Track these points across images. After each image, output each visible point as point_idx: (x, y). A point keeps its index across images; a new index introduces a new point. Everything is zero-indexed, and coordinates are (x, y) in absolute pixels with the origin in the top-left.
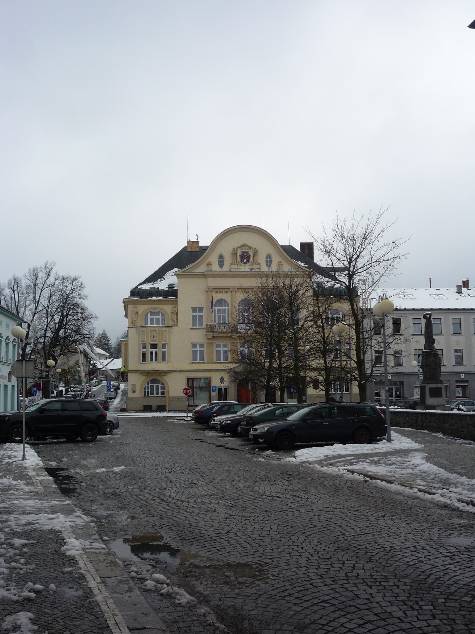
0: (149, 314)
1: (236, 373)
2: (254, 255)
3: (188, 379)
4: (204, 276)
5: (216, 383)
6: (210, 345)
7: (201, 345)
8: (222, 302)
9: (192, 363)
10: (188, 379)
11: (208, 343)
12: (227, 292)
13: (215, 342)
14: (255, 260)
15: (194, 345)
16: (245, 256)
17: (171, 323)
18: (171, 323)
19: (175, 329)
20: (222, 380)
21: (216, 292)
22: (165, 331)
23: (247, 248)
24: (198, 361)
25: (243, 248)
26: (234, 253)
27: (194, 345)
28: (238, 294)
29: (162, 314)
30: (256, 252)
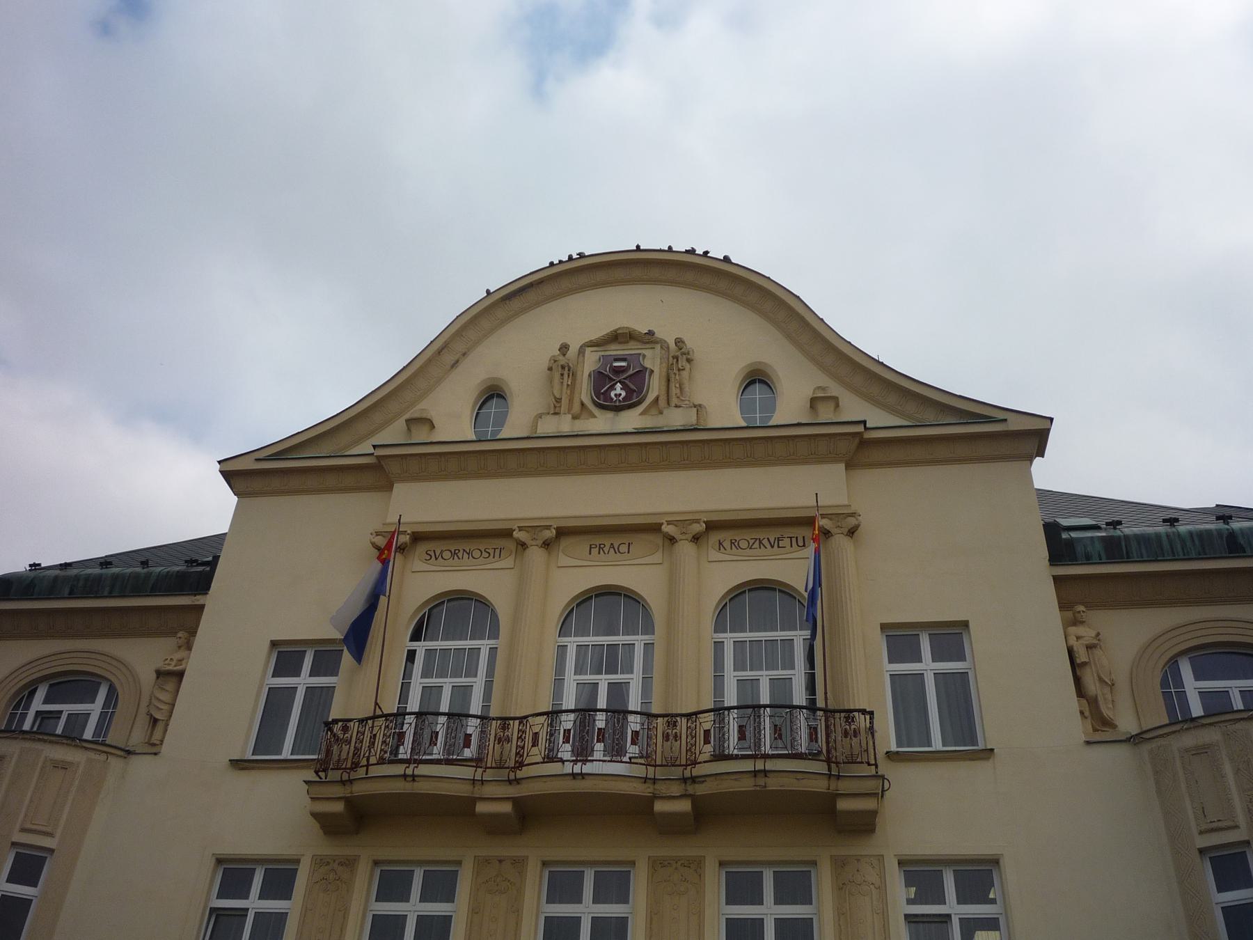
0: (41, 694)
2: (670, 368)
4: (379, 473)
6: (335, 874)
7: (280, 880)
8: (460, 611)
11: (320, 861)
13: (368, 852)
14: (674, 391)
15: (234, 875)
16: (618, 371)
17: (137, 738)
18: (137, 738)
19: (141, 766)
21: (431, 556)
22: (63, 766)
23: (632, 344)
25: (613, 347)
26: (562, 368)
27: (234, 875)
28: (564, 560)
29: (112, 691)
30: (680, 357)
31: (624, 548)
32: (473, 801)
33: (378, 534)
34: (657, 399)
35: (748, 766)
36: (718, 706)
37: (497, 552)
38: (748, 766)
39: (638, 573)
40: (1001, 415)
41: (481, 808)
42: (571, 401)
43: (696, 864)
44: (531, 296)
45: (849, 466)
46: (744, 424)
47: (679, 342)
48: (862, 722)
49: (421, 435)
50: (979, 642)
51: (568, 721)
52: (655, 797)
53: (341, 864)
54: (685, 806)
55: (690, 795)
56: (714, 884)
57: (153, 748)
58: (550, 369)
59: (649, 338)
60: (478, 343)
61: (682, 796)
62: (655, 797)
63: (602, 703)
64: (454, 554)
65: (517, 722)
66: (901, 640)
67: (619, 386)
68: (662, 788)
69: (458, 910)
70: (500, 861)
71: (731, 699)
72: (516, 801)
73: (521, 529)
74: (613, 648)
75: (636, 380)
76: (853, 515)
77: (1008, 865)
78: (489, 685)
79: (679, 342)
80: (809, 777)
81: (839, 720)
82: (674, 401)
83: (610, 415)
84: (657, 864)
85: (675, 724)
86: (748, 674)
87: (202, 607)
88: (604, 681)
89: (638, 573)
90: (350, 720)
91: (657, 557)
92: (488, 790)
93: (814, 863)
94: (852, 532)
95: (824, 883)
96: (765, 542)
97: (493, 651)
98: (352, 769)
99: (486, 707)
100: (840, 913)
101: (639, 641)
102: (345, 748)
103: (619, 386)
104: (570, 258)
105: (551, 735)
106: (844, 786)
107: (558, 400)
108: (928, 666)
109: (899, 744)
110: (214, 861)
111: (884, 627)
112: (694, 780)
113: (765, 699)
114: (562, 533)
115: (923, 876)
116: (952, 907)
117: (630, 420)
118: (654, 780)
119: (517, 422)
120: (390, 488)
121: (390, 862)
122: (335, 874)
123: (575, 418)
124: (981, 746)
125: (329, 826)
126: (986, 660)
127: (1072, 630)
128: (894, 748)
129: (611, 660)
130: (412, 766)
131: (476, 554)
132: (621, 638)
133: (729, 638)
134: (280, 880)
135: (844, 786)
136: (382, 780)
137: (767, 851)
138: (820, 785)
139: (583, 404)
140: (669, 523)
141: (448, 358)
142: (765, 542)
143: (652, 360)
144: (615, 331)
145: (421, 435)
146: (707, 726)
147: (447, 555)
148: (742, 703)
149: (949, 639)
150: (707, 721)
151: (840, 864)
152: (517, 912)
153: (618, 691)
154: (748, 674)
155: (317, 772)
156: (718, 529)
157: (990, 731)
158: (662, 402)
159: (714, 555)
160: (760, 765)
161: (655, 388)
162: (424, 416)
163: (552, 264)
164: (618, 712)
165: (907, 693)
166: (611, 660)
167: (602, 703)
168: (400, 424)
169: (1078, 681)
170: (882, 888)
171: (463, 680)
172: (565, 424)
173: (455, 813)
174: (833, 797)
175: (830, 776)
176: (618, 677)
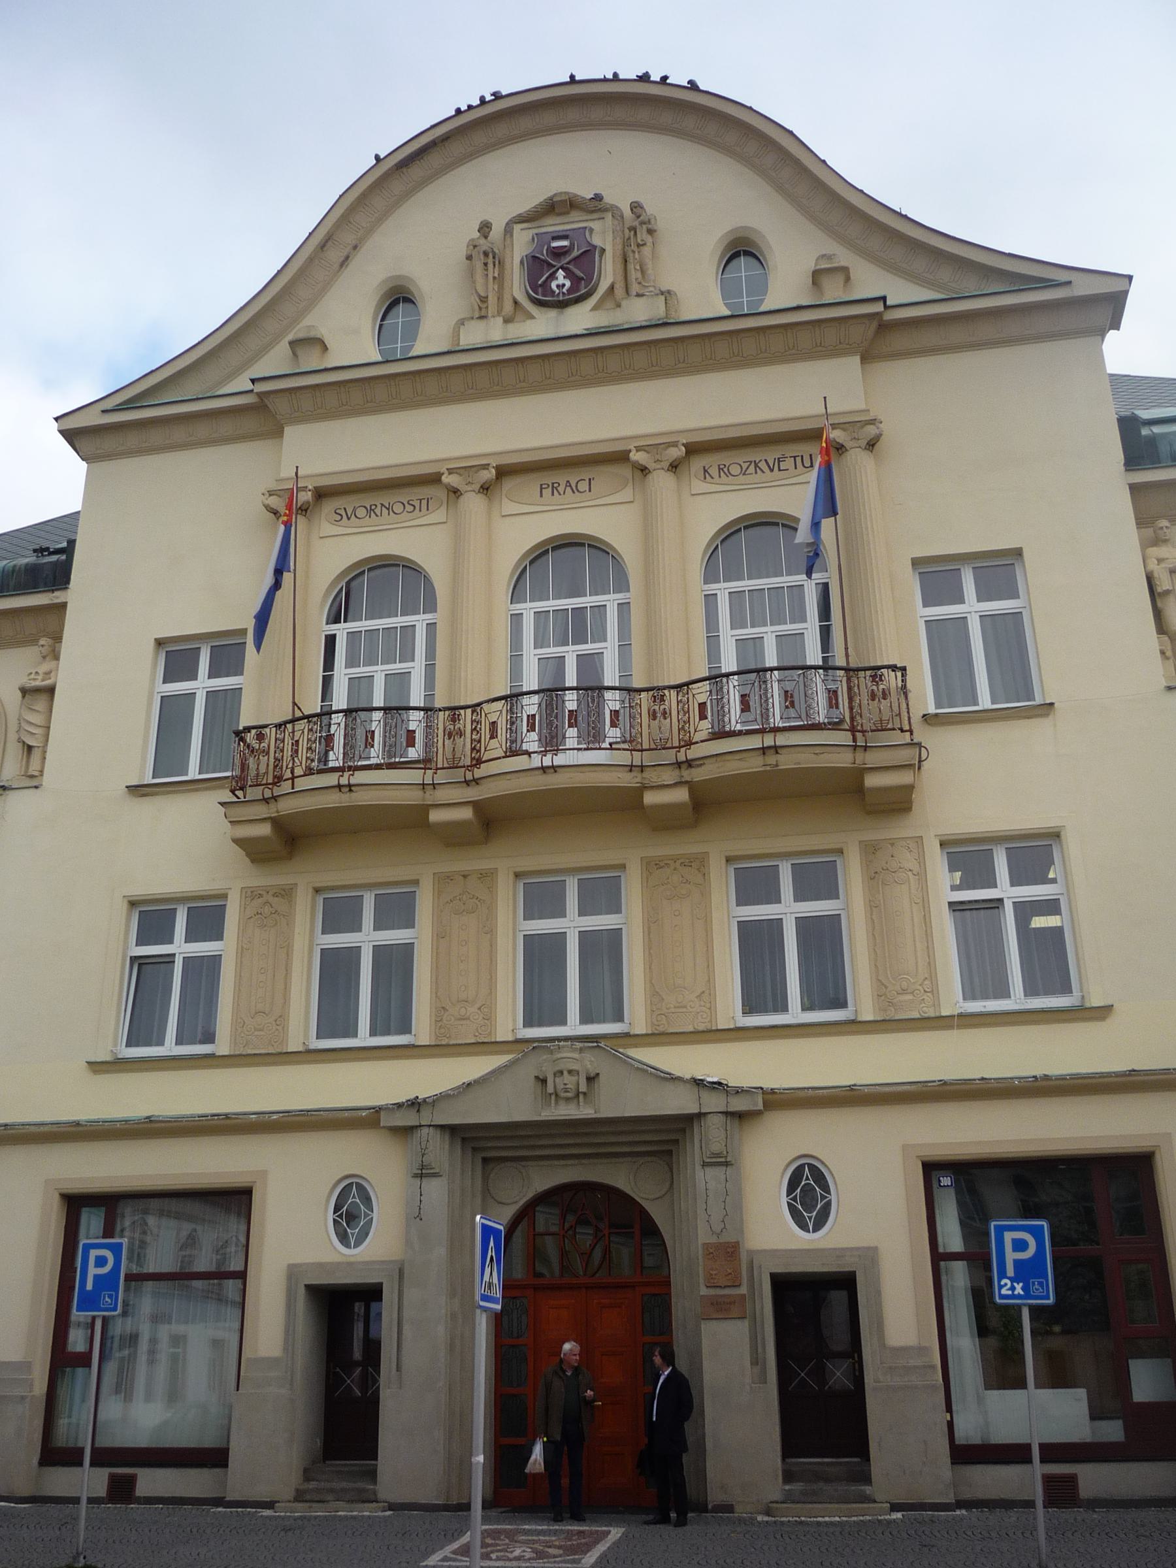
1: (464, 1136)
2: (626, 243)
3: (75, 1204)
5: (293, 1239)
6: (270, 908)
7: (207, 919)
9: (118, 1065)
10: (75, 1204)
11: (250, 894)
12: (427, 504)
13: (305, 878)
14: (634, 275)
15: (152, 918)
16: (558, 253)
20: (350, 1210)
21: (342, 516)
23: (575, 215)
24: (169, 1047)
25: (550, 220)
26: (484, 255)
27: (152, 918)
28: (509, 507)
30: (639, 228)
31: (583, 486)
32: (425, 809)
33: (271, 493)
34: (612, 288)
35: (755, 742)
36: (714, 672)
37: (424, 502)
38: (755, 742)
39: (603, 516)
40: (1063, 276)
41: (435, 816)
42: (500, 299)
43: (699, 863)
44: (435, 159)
45: (864, 359)
46: (727, 313)
47: (636, 207)
48: (892, 680)
49: (311, 360)
50: (1036, 574)
51: (531, 705)
52: (644, 788)
53: (275, 895)
54: (681, 795)
55: (687, 782)
56: (722, 885)
57: (33, 780)
58: (469, 258)
59: (596, 205)
60: (370, 231)
61: (676, 784)
62: (644, 788)
63: (571, 680)
64: (370, 511)
65: (469, 711)
66: (938, 576)
67: (561, 273)
68: (652, 777)
69: (420, 936)
70: (465, 876)
71: (729, 663)
72: (476, 805)
73: (451, 471)
74: (579, 612)
75: (582, 263)
76: (873, 422)
77: (1072, 843)
78: (430, 669)
79: (636, 207)
80: (831, 751)
81: (864, 679)
82: (635, 288)
83: (552, 313)
84: (651, 866)
85: (662, 699)
86: (749, 632)
87: (64, 606)
88: (571, 654)
89: (603, 516)
90: (266, 726)
91: (626, 494)
92: (442, 795)
93: (840, 852)
94: (871, 445)
95: (852, 875)
96: (763, 465)
97: (431, 627)
98: (274, 784)
99: (429, 697)
100: (872, 906)
101: (611, 601)
102: (264, 759)
103: (561, 273)
104: (483, 100)
105: (512, 723)
106: (872, 759)
107: (484, 299)
108: (972, 608)
109: (938, 706)
110: (125, 905)
111: (916, 562)
112: (689, 763)
113: (771, 660)
114: (503, 472)
115: (969, 857)
116: (1006, 890)
117: (580, 318)
118: (642, 768)
119: (434, 332)
120: (278, 433)
121: (333, 889)
122: (270, 908)
123: (507, 321)
124: (1038, 700)
125: (256, 852)
126: (1043, 597)
127: (1154, 552)
128: (932, 709)
129: (579, 626)
130: (346, 774)
131: (398, 508)
132: (588, 599)
133: (723, 590)
134: (207, 919)
135: (872, 759)
136: (310, 795)
137: (783, 840)
138: (844, 760)
139: (516, 302)
140: (638, 449)
141: (334, 255)
142: (763, 465)
143: (603, 234)
144: (551, 198)
145: (311, 360)
146: (702, 698)
147: (361, 512)
148: (742, 668)
149: (1000, 569)
150: (702, 692)
151: (870, 850)
152: (491, 932)
153: (589, 663)
154: (749, 632)
155: (233, 792)
156: (700, 452)
157: (1049, 682)
158: (619, 291)
159: (699, 486)
160: (769, 740)
161: (608, 272)
162: (312, 334)
163: (458, 111)
164: (592, 689)
165: (947, 640)
166: (579, 626)
167: (571, 680)
168: (283, 347)
169: (1158, 614)
170: (922, 876)
171: (398, 665)
172: (496, 331)
173: (406, 824)
174: (860, 772)
175: (855, 747)
176: (589, 648)
